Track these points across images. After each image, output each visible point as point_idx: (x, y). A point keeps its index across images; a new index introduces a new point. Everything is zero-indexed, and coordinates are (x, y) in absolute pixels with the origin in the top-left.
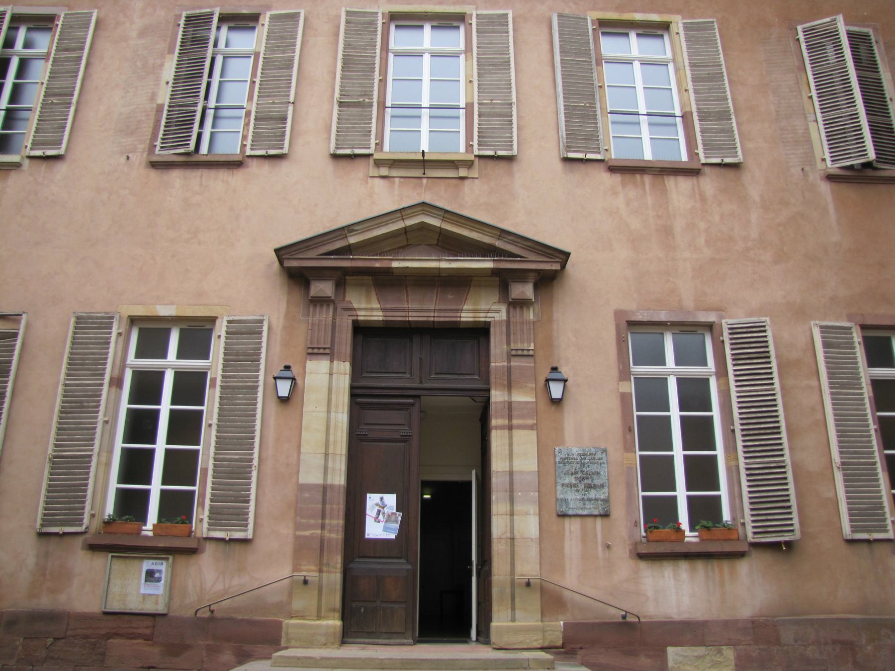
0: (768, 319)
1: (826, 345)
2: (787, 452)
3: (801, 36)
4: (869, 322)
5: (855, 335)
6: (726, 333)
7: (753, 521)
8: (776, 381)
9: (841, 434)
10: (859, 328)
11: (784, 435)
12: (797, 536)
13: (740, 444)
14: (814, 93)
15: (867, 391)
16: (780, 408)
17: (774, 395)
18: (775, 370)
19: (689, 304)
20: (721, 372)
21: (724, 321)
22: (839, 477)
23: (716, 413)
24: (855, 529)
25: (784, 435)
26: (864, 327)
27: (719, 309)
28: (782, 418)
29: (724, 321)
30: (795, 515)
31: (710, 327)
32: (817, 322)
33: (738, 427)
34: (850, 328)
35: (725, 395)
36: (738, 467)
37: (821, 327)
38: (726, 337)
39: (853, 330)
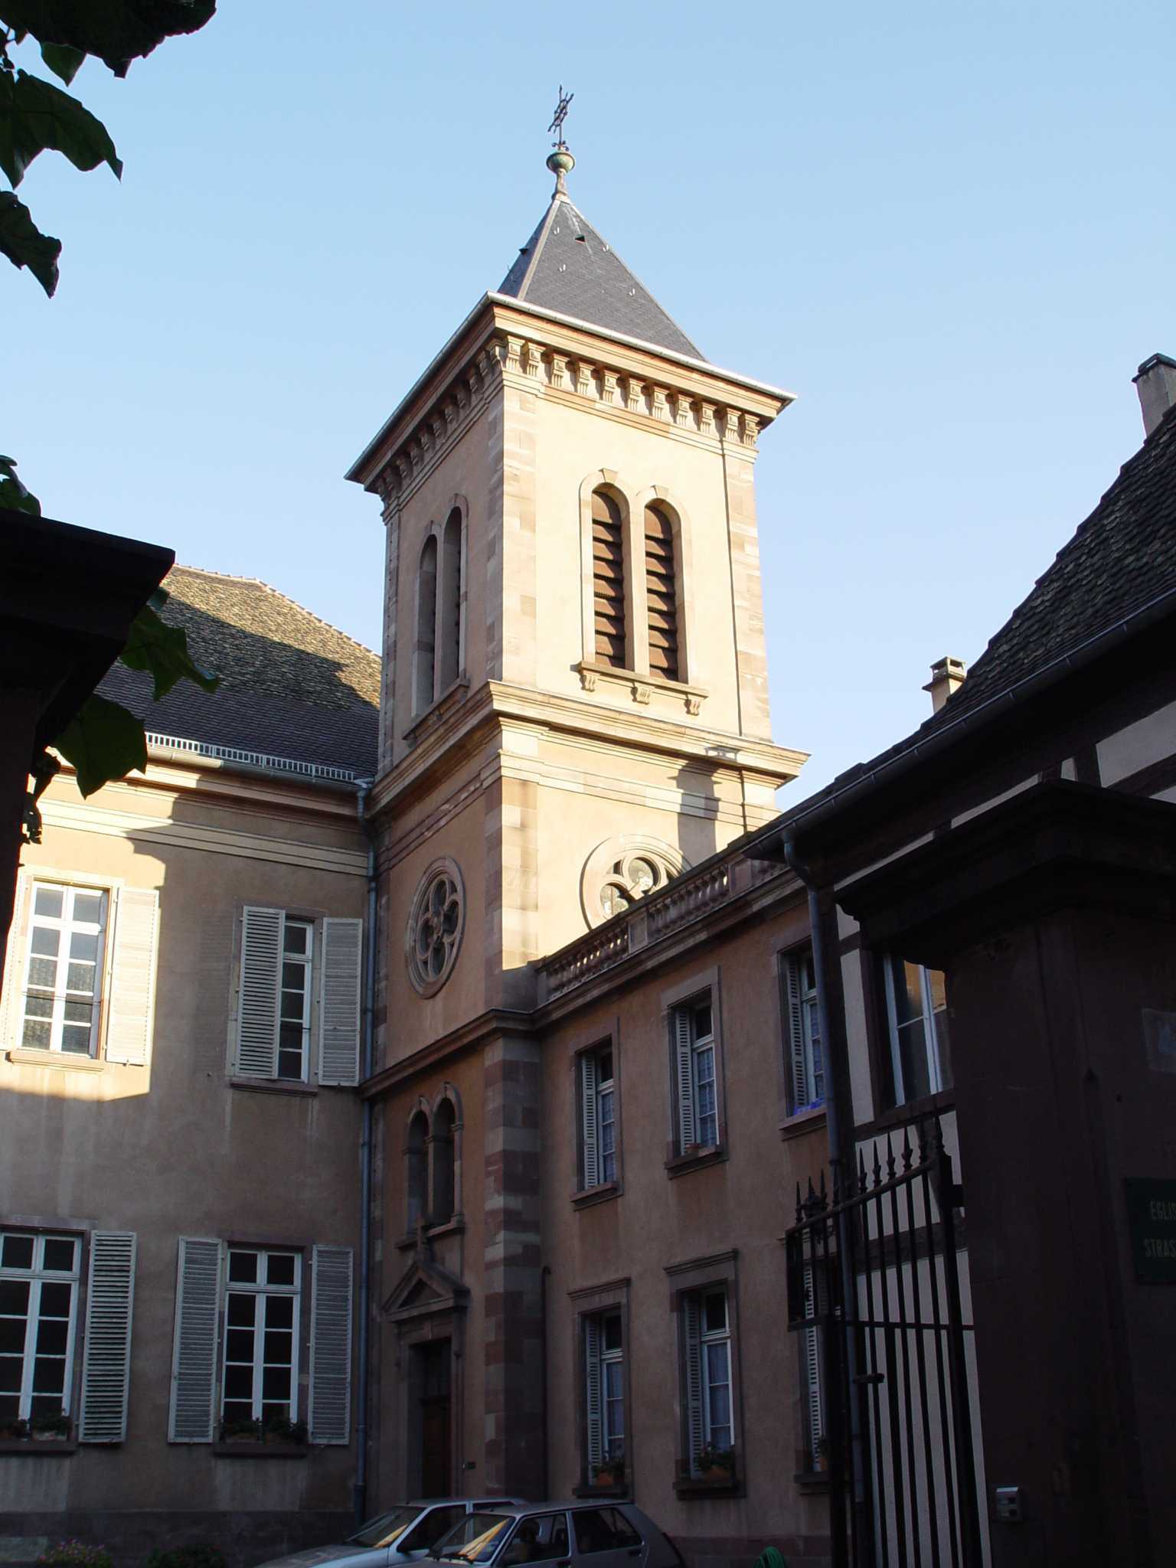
0: (135, 1234)
1: (188, 1261)
2: (127, 1362)
3: (245, 919)
4: (237, 1238)
5: (220, 1251)
6: (93, 1243)
7: (87, 1423)
8: (131, 1295)
9: (185, 1346)
10: (226, 1244)
11: (128, 1346)
12: (122, 1438)
13: (86, 1351)
14: (242, 989)
15: (221, 1304)
16: (129, 1320)
17: (126, 1307)
18: (132, 1284)
19: (64, 1210)
20: (83, 1281)
21: (93, 1232)
22: (174, 1384)
23: (72, 1320)
24: (178, 1434)
25: (128, 1346)
26: (232, 1244)
27: (93, 1218)
28: (129, 1331)
29: (93, 1232)
30: (124, 1420)
31: (81, 1234)
32: (185, 1238)
33: (88, 1335)
34: (216, 1245)
35: (82, 1302)
36: (81, 1372)
37: (187, 1243)
38: (92, 1247)
39: (220, 1247)
